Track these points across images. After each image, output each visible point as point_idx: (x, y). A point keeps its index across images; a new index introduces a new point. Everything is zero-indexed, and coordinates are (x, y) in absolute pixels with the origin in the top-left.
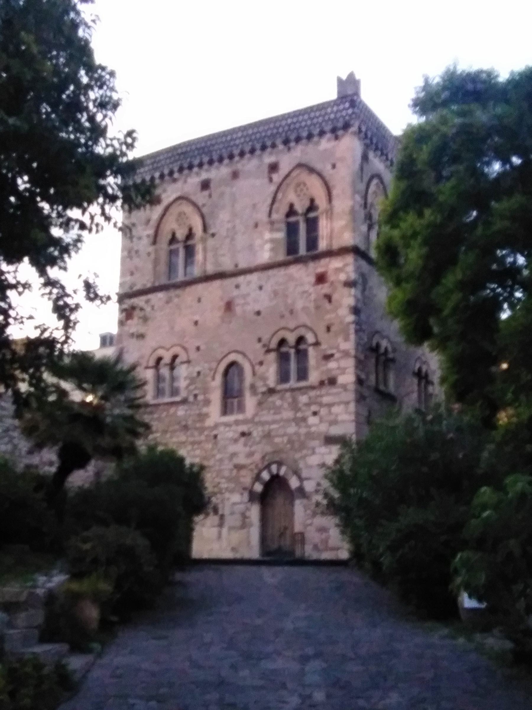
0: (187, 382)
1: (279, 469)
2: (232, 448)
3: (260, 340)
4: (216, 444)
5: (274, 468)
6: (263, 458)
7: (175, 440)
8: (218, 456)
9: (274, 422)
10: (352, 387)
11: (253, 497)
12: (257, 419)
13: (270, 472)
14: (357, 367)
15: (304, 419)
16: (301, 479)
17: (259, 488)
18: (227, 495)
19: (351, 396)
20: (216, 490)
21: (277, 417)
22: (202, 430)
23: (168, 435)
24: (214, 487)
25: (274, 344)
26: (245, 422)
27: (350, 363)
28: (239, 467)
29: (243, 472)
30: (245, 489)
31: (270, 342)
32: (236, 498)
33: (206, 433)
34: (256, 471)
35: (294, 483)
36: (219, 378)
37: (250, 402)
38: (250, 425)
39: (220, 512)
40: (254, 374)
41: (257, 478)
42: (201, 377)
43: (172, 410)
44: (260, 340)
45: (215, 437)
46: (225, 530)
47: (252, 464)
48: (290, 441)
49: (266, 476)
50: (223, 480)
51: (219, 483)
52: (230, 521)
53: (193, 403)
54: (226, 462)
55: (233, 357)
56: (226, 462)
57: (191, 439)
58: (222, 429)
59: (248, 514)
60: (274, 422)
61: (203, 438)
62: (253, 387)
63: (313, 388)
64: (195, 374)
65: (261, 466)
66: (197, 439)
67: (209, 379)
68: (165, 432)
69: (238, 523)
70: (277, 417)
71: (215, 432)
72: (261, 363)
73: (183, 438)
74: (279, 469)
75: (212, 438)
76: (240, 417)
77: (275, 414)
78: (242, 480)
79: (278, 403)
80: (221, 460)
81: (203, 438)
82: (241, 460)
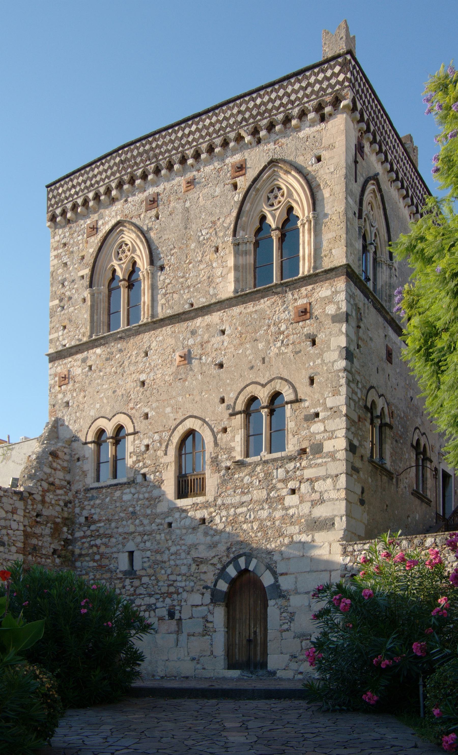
0: (134, 458)
1: (248, 563)
2: (190, 539)
3: (223, 400)
4: (170, 533)
5: (242, 562)
6: (228, 549)
7: (120, 530)
8: (173, 549)
9: (242, 504)
10: (342, 455)
11: (216, 597)
12: (219, 502)
13: (237, 566)
14: (348, 429)
15: (281, 499)
16: (274, 573)
17: (223, 586)
18: (185, 595)
19: (340, 467)
20: (172, 589)
21: (246, 498)
22: (153, 517)
23: (113, 525)
24: (169, 586)
25: (240, 406)
26: (206, 505)
27: (340, 425)
28: (199, 562)
29: (204, 568)
30: (206, 587)
31: (235, 403)
32: (196, 598)
33: (158, 521)
34: (219, 566)
35: (267, 580)
36: (172, 451)
37: (212, 481)
38: (212, 509)
39: (177, 616)
40: (216, 444)
41: (222, 574)
42: (151, 451)
43: (118, 494)
44: (223, 400)
45: (170, 525)
46: (183, 637)
47: (214, 557)
48: (262, 528)
49: (232, 572)
50: (179, 578)
51: (174, 581)
52: (187, 626)
53: (141, 485)
54: (183, 555)
55: (190, 424)
56: (183, 555)
57: (141, 529)
58: (177, 515)
59: (210, 618)
60: (242, 504)
61: (154, 527)
62: (215, 461)
63: (291, 459)
64: (143, 448)
65: (225, 560)
66: (148, 528)
67: (160, 453)
68: (109, 521)
69: (200, 630)
70: (246, 498)
71: (169, 520)
72: (225, 430)
73: (132, 529)
74: (248, 563)
75: (166, 526)
76: (200, 499)
77: (243, 493)
78: (203, 576)
79: (247, 480)
80: (176, 553)
81: (154, 527)
82: (203, 552)
